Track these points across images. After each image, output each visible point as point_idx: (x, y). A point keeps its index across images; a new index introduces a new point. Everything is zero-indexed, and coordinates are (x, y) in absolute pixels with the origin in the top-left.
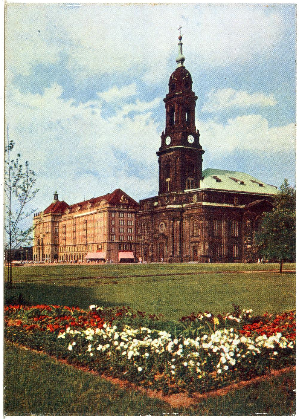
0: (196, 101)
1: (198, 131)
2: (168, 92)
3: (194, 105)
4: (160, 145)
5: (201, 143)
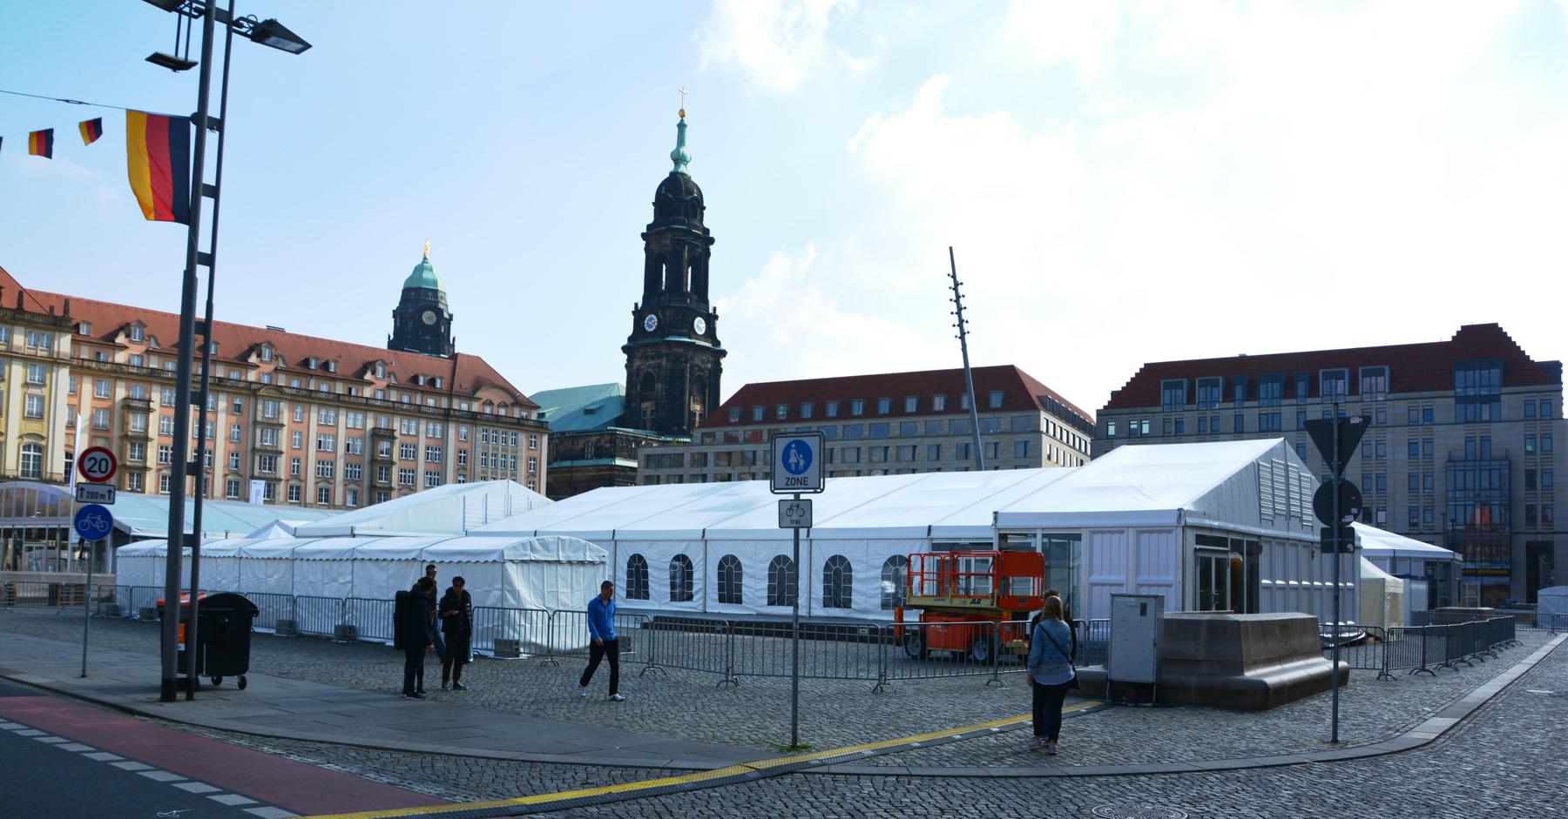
0: (711, 247)
1: (715, 309)
2: (651, 220)
3: (708, 254)
4: (630, 331)
5: (719, 336)
